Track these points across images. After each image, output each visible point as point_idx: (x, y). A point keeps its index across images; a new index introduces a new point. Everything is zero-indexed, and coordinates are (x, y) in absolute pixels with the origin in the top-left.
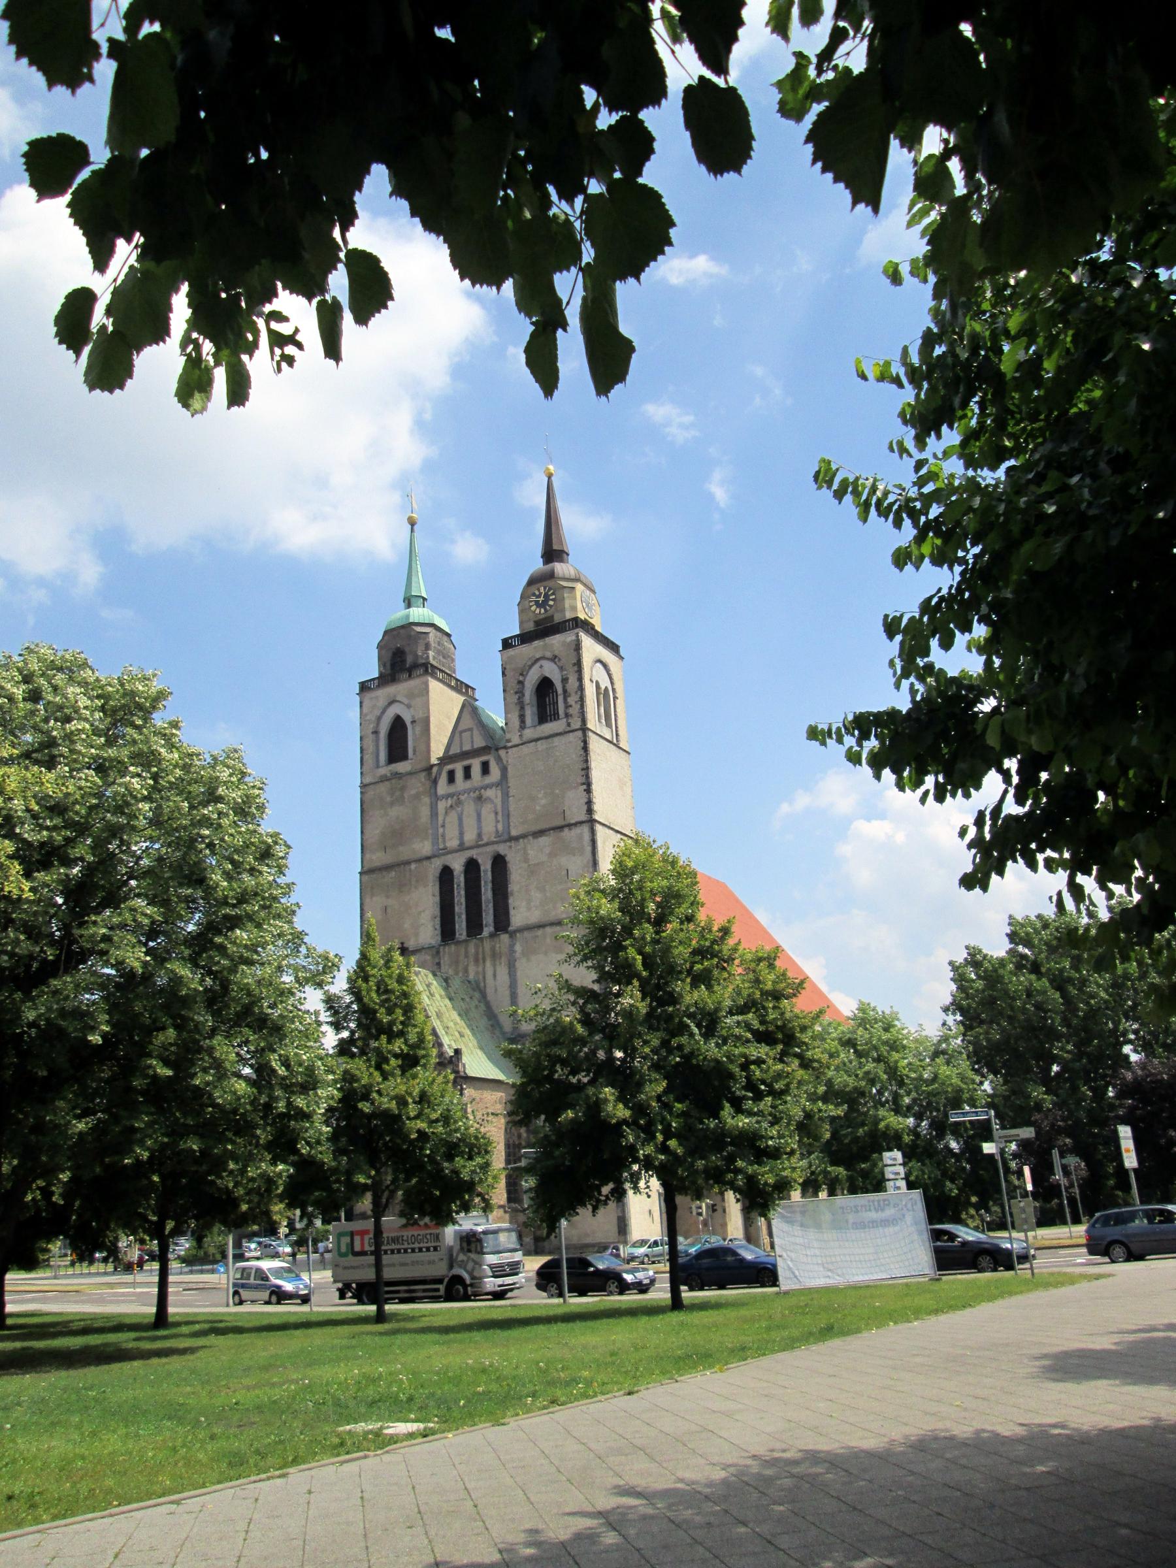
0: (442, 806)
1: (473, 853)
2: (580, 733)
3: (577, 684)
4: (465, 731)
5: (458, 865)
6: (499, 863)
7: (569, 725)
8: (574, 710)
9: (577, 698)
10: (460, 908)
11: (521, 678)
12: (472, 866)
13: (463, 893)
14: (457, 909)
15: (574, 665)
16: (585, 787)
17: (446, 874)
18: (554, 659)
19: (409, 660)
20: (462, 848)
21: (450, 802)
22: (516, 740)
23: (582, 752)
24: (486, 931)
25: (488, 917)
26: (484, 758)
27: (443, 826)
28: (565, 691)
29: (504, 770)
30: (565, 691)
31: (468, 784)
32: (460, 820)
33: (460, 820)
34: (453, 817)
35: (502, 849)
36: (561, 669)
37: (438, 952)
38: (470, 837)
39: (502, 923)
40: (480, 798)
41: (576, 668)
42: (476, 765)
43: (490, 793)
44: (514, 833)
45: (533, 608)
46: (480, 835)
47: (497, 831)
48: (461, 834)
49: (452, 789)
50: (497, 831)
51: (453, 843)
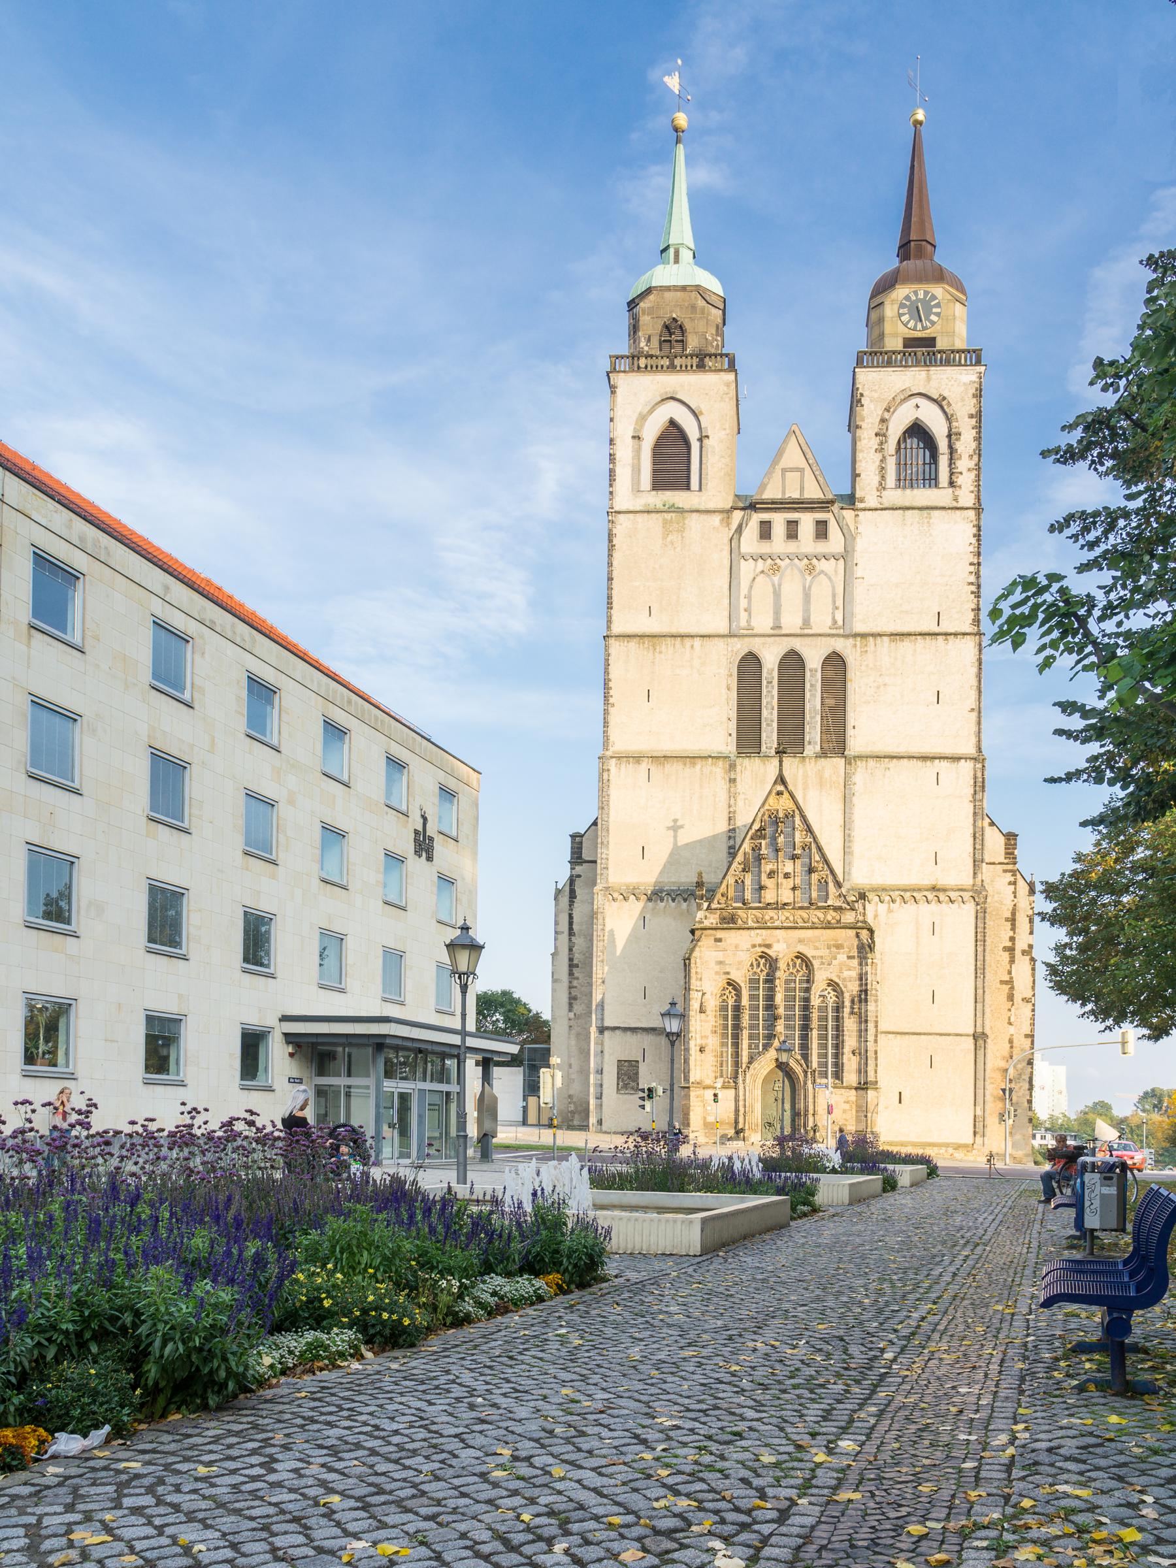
0: (746, 569)
1: (798, 645)
2: (971, 514)
3: (974, 445)
4: (792, 470)
5: (771, 659)
6: (835, 663)
7: (956, 500)
8: (966, 480)
9: (972, 464)
10: (770, 714)
11: (887, 416)
12: (792, 662)
13: (775, 692)
14: (765, 713)
15: (971, 416)
16: (973, 588)
17: (750, 665)
18: (939, 402)
19: (693, 343)
20: (777, 632)
21: (760, 564)
22: (871, 501)
23: (974, 541)
24: (810, 750)
25: (813, 732)
26: (821, 516)
27: (749, 597)
28: (952, 449)
29: (849, 538)
30: (952, 449)
31: (792, 547)
32: (777, 594)
33: (777, 594)
34: (764, 586)
35: (840, 645)
36: (949, 418)
37: (732, 767)
38: (791, 621)
39: (836, 742)
40: (811, 569)
41: (973, 421)
42: (807, 522)
43: (823, 565)
44: (859, 628)
45: (905, 318)
46: (806, 622)
47: (835, 622)
48: (777, 614)
49: (765, 548)
50: (835, 622)
51: (763, 623)
